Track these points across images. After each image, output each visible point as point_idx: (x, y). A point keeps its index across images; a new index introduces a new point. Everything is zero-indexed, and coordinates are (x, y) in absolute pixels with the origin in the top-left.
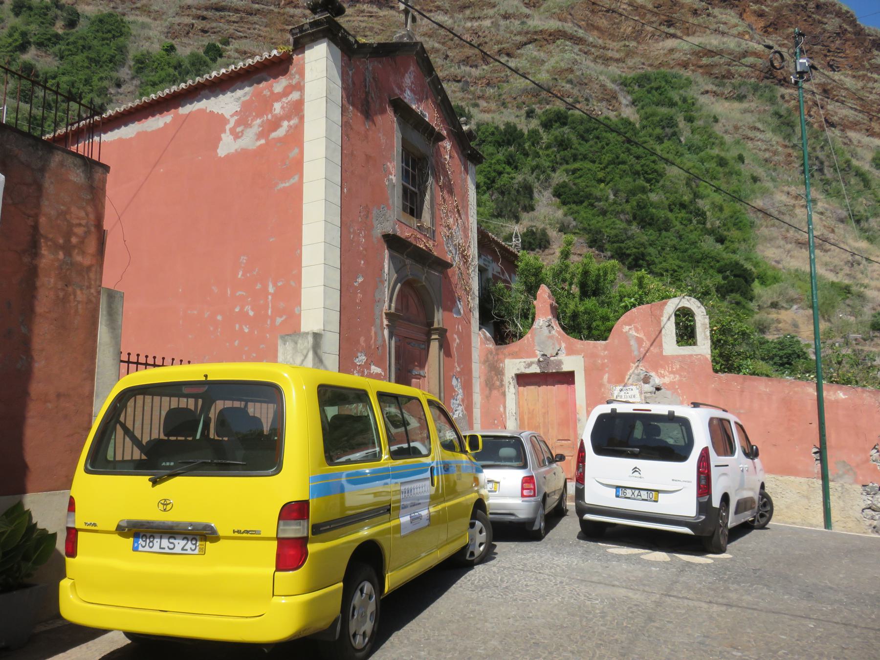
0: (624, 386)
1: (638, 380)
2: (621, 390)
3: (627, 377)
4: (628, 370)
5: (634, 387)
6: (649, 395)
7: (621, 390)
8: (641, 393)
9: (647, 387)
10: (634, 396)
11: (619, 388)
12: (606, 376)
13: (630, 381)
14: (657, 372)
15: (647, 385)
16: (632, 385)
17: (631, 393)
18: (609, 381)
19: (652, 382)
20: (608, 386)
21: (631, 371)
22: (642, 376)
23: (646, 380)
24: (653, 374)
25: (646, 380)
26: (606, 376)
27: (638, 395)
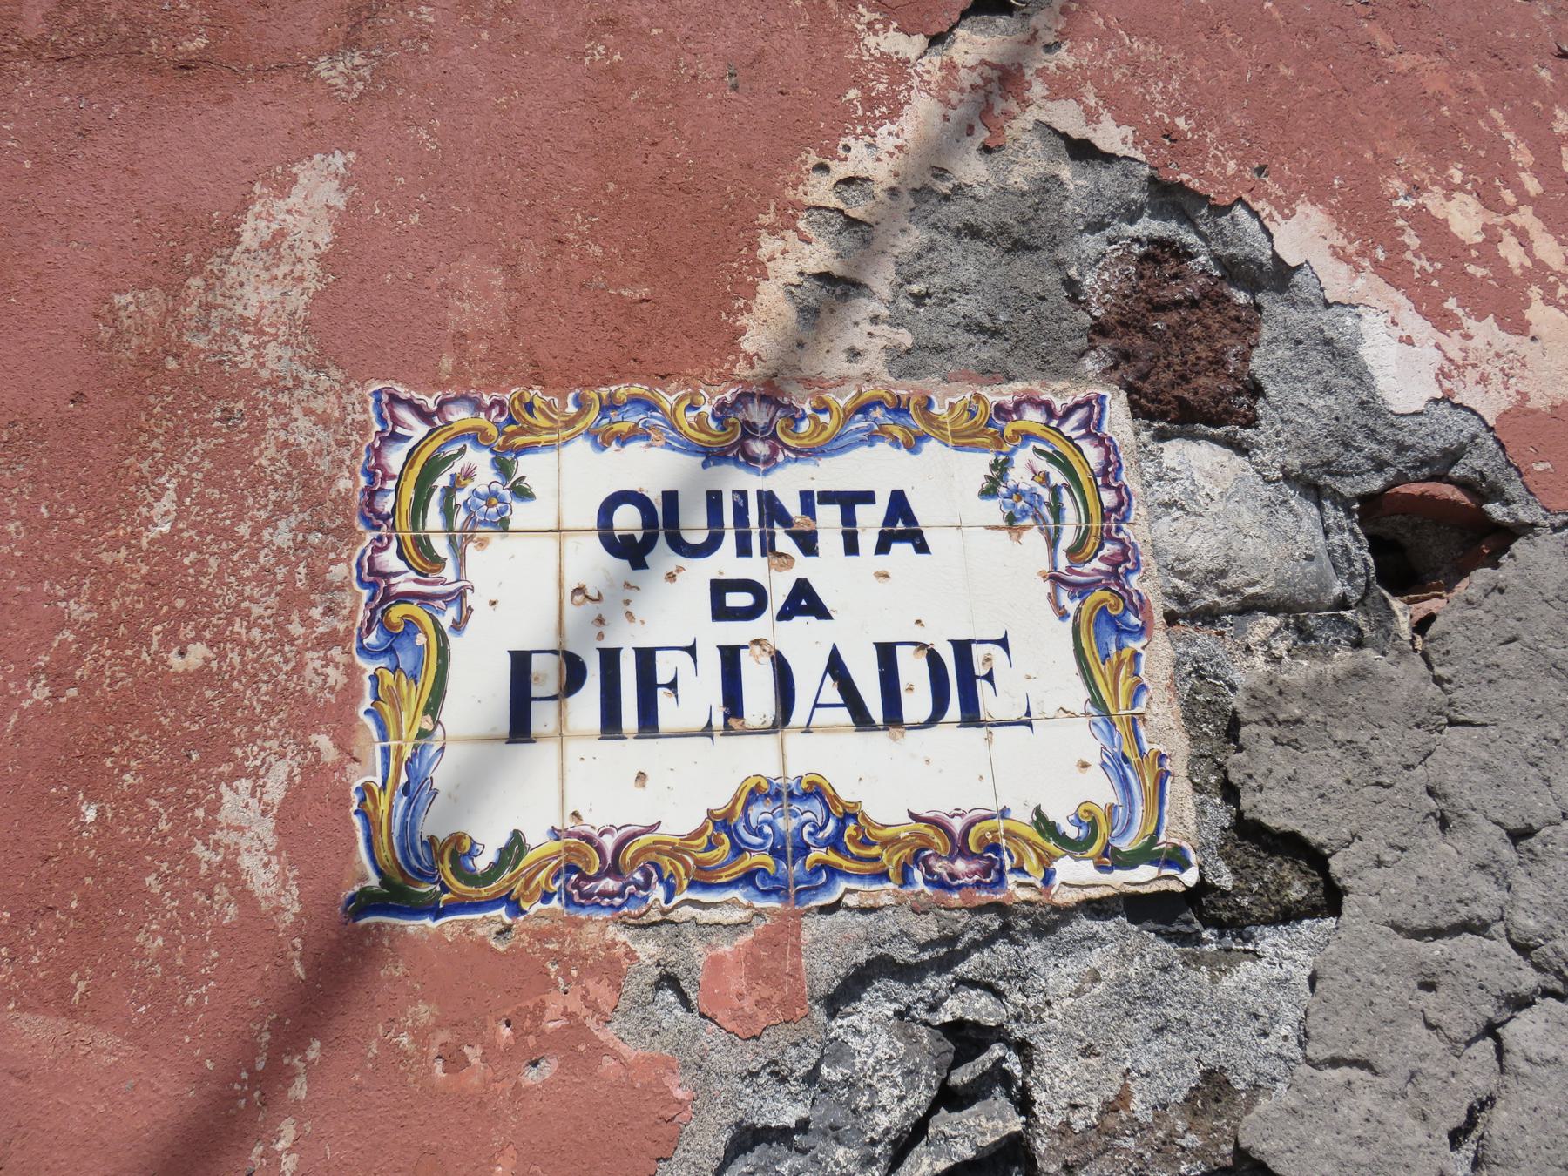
0: (730, 444)
1: (1010, 338)
2: (644, 535)
3: (795, 257)
4: (822, 132)
5: (944, 481)
6: (1253, 659)
7: (644, 535)
8: (1103, 612)
9: (1211, 505)
10: (959, 681)
11: (575, 477)
12: (308, 203)
13: (864, 346)
14: (1367, 225)
15: (1197, 460)
16: (901, 419)
17: (870, 601)
18: (354, 319)
19: (1297, 407)
20: (316, 421)
21: (875, 157)
22: (1098, 268)
23: (1186, 346)
24: (1301, 236)
25: (1186, 346)
26: (308, 203)
27: (1039, 663)
